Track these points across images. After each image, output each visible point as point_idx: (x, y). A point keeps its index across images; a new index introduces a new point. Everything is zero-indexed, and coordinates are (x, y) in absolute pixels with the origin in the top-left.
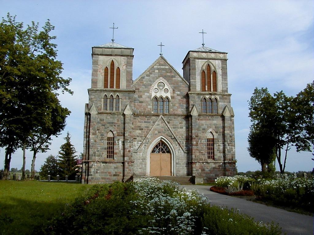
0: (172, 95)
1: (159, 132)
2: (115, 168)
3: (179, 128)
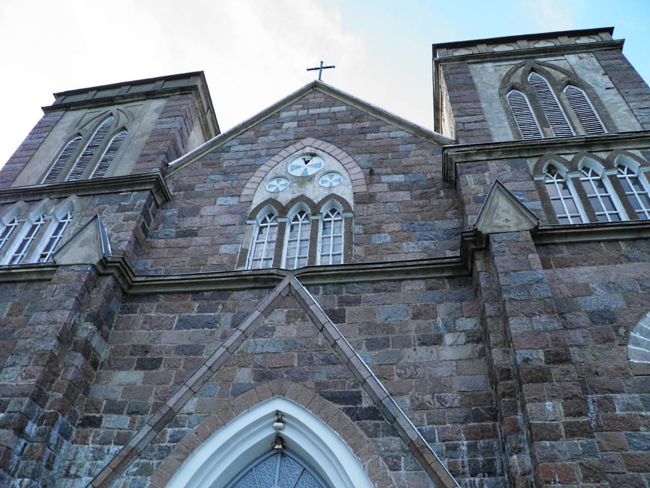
0: (363, 189)
1: (263, 376)
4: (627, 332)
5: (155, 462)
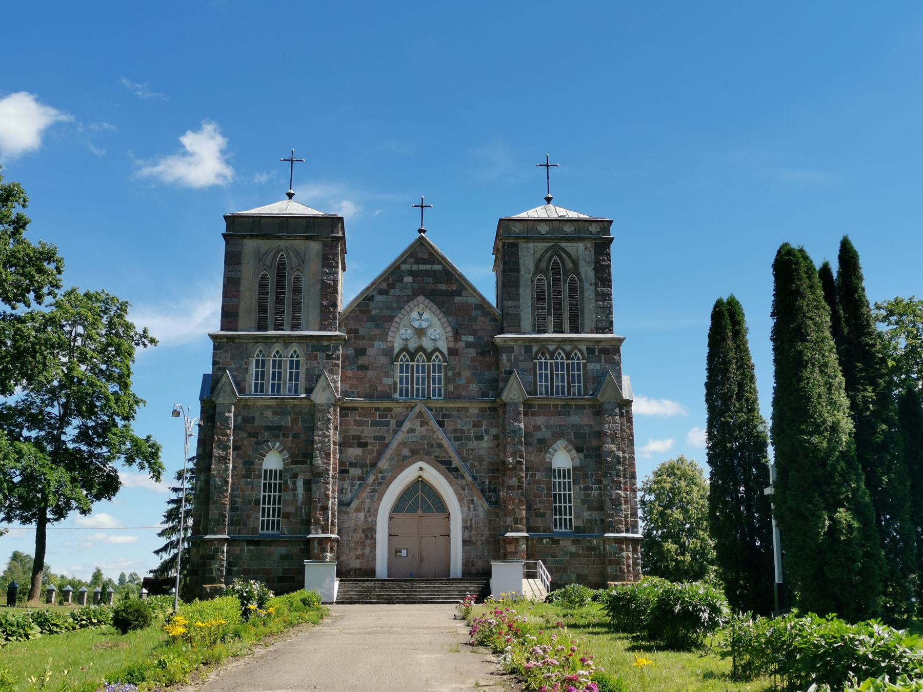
0: (452, 345)
2: (284, 557)
3: (470, 440)
4: (548, 449)
5: (377, 488)
